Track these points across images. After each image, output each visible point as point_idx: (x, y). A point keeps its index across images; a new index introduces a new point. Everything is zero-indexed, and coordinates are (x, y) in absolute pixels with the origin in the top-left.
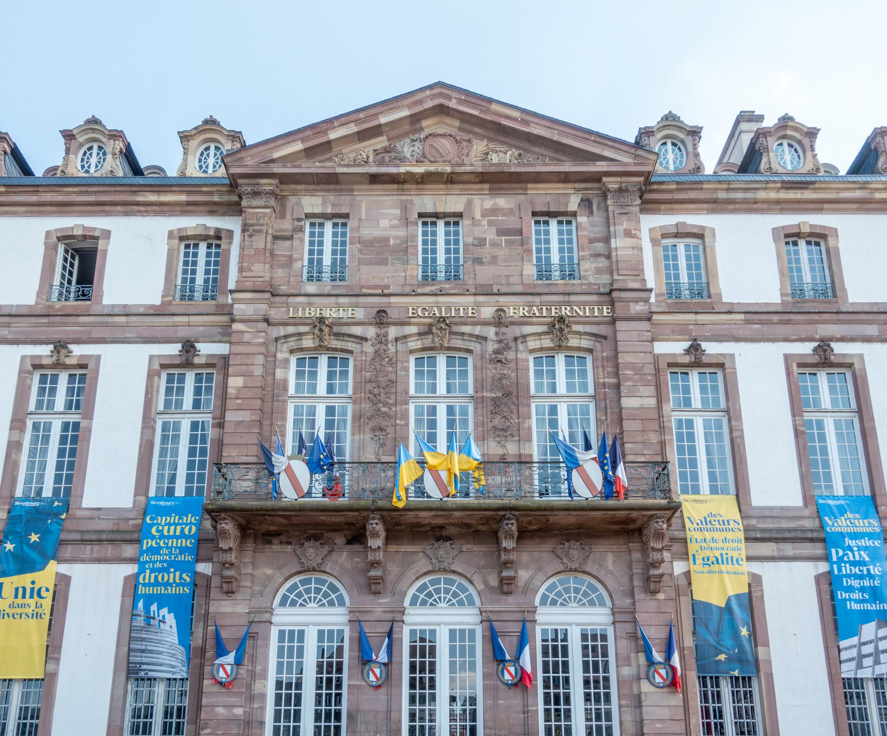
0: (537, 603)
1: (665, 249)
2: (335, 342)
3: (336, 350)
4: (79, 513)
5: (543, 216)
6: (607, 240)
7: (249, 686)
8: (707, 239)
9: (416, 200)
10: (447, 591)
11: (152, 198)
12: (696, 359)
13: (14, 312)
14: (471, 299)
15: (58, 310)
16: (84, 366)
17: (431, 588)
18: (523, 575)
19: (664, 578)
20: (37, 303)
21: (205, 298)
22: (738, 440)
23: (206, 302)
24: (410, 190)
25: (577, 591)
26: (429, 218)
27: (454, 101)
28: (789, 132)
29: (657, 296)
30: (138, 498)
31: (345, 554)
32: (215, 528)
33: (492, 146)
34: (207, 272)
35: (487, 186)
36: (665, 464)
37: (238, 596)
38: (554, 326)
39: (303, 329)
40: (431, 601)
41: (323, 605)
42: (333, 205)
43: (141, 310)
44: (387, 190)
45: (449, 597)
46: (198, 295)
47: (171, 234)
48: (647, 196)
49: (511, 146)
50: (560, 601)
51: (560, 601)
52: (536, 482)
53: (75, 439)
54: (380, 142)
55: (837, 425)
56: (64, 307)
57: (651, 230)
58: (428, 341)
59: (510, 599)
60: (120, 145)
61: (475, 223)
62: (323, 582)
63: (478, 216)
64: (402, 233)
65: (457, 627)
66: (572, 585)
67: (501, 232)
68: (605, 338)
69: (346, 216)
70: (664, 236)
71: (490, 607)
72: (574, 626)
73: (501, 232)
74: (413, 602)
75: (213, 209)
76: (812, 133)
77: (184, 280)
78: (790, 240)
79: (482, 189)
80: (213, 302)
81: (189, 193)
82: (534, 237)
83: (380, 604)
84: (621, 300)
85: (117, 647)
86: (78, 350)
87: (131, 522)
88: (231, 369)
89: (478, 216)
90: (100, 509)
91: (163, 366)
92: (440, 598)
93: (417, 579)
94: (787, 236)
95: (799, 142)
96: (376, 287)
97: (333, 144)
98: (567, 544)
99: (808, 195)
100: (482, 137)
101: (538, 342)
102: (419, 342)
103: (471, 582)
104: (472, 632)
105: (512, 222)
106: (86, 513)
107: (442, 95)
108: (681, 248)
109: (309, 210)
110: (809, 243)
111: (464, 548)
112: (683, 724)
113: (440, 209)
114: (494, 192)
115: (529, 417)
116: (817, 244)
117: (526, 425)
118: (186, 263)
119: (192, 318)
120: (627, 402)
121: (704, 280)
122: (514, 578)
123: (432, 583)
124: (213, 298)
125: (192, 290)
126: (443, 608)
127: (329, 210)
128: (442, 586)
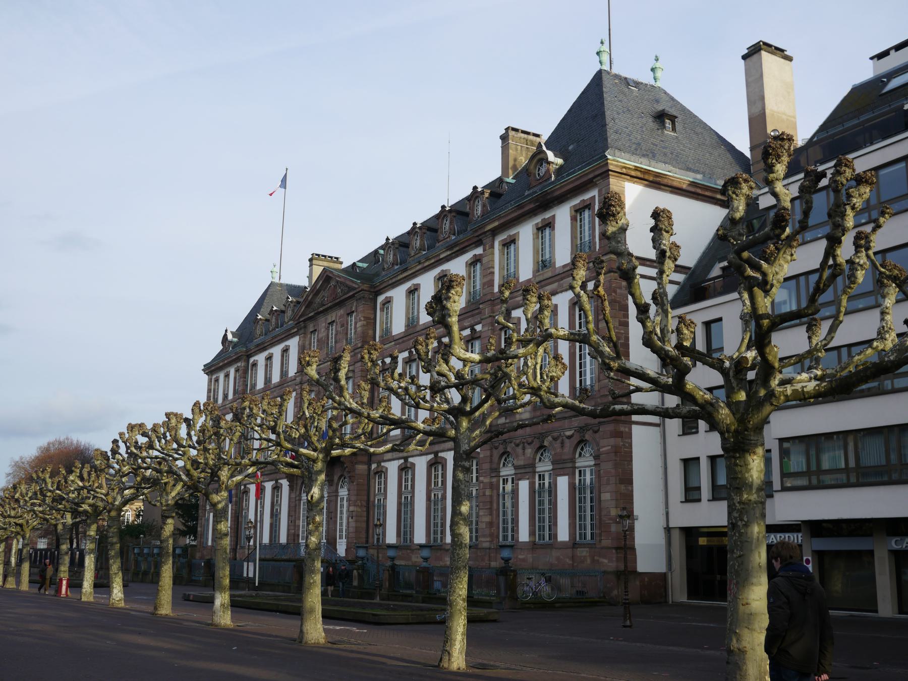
26: (332, 323)
99: (410, 272)
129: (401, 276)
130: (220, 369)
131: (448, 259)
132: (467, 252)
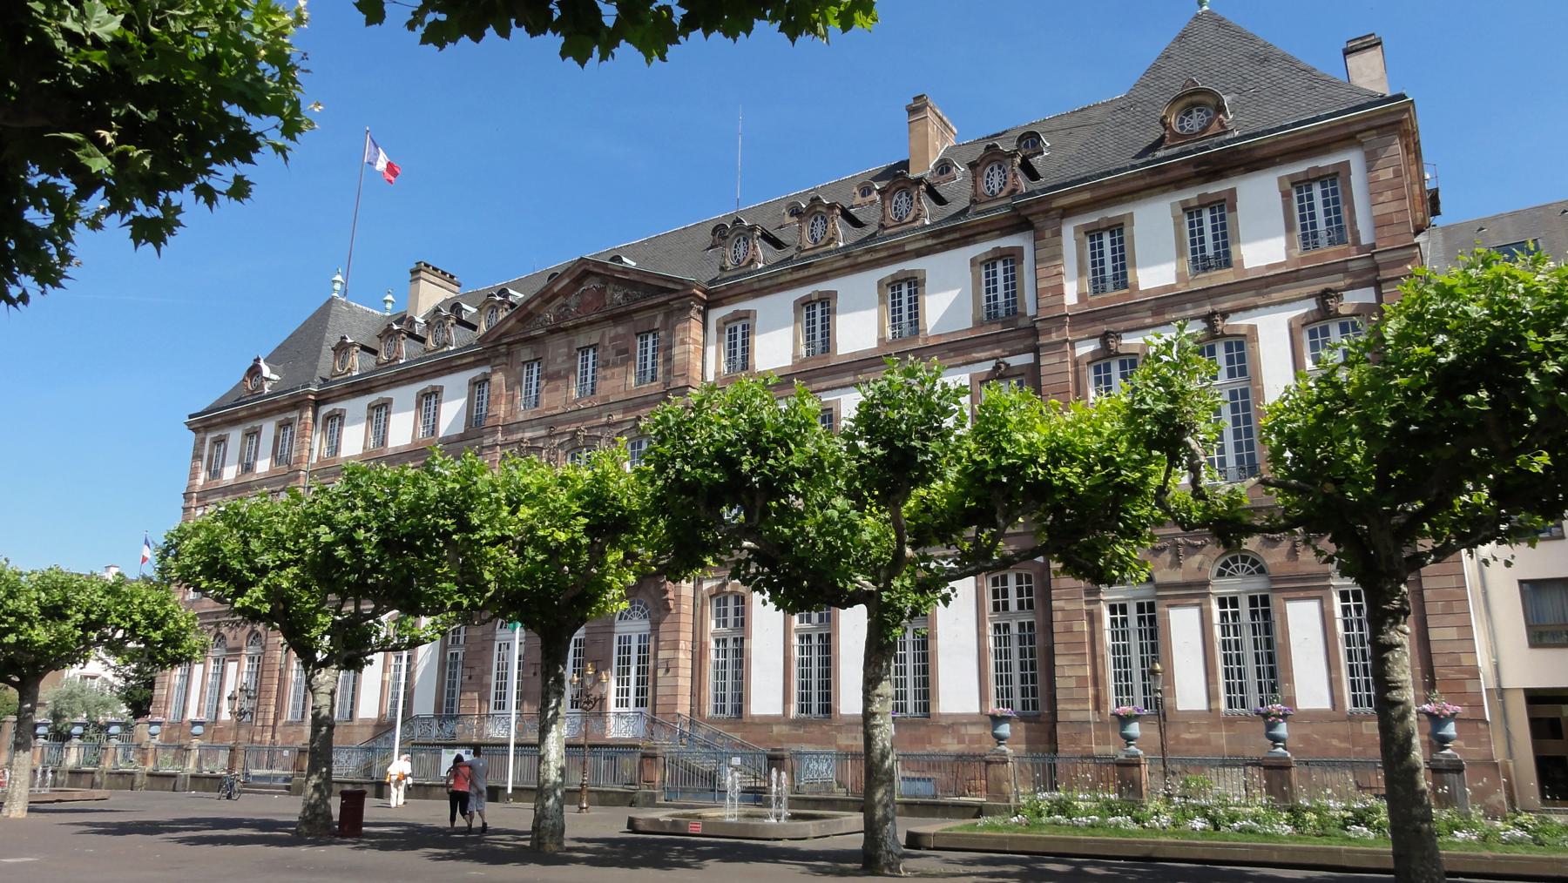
5: (642, 335)
26: (584, 350)
99: (813, 271)
114: (615, 326)
129: (789, 278)
130: (234, 422)
131: (919, 253)
132: (975, 242)
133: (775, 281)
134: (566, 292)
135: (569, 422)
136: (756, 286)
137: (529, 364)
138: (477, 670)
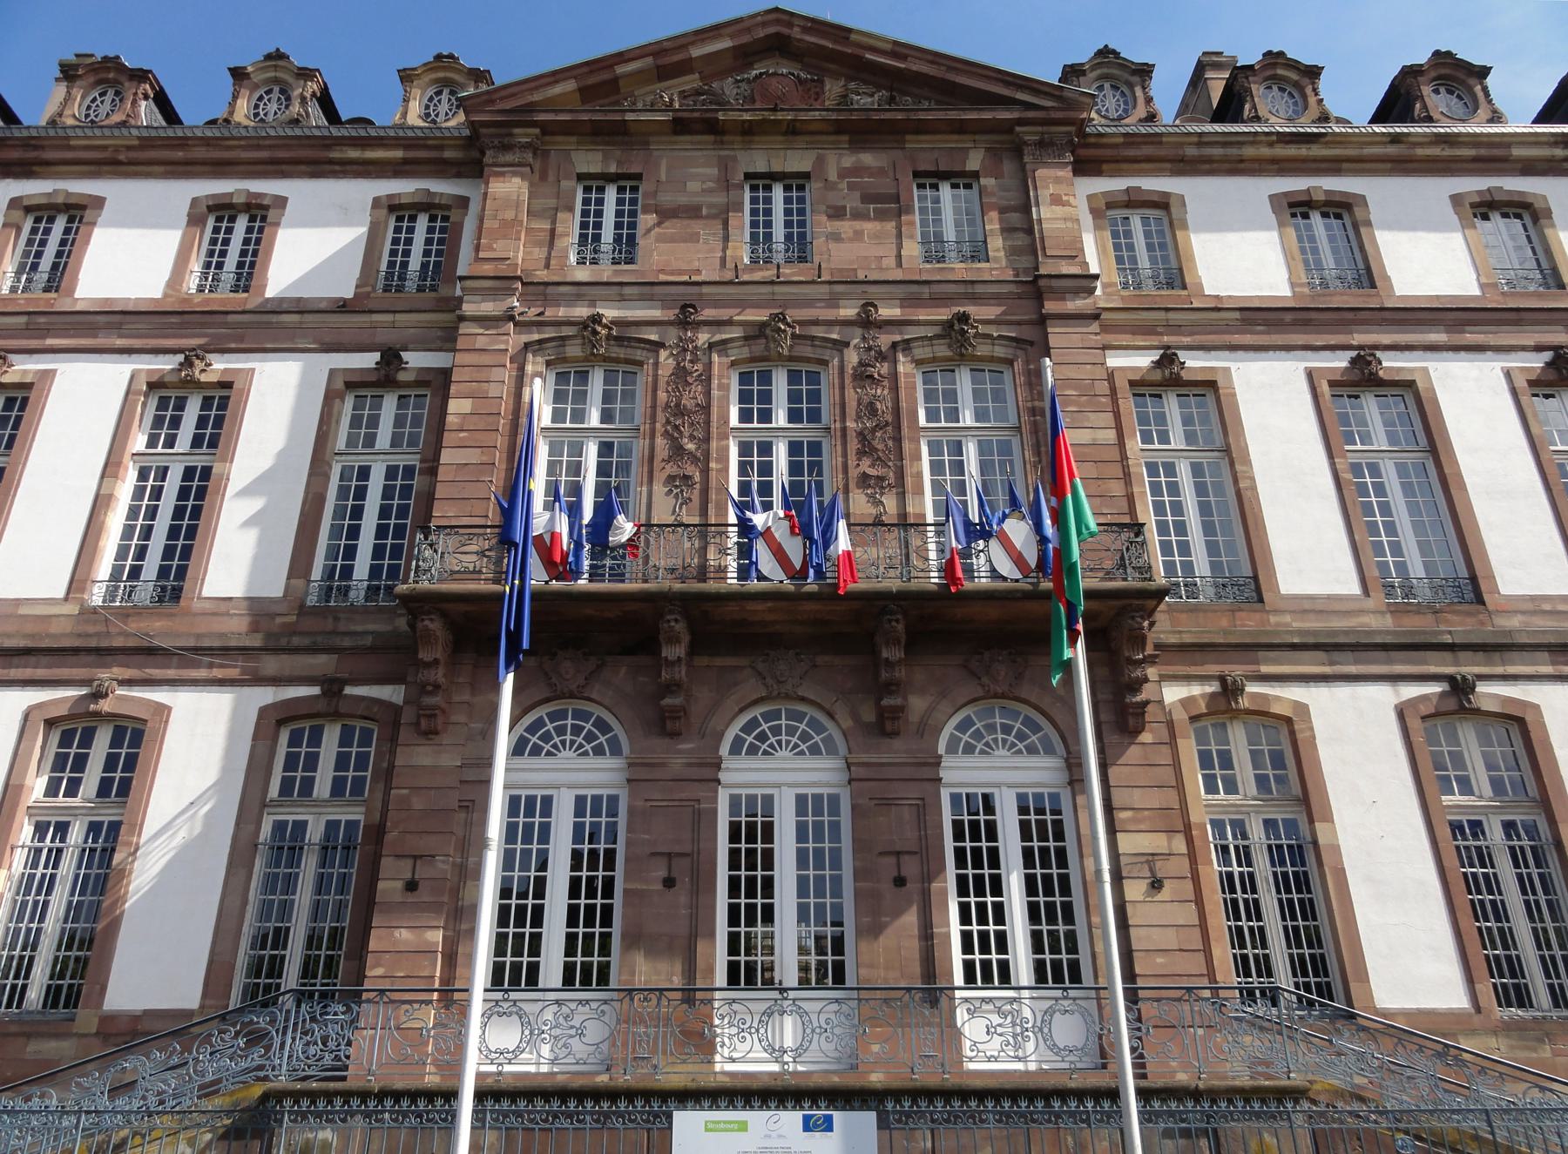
0: (941, 749)
1: (1114, 223)
2: (616, 349)
3: (617, 361)
4: (197, 605)
5: (930, 178)
6: (1026, 209)
7: (456, 892)
8: (1173, 210)
9: (742, 156)
10: (791, 731)
11: (353, 154)
12: (1167, 377)
13: (130, 308)
14: (826, 288)
15: (199, 304)
16: (228, 385)
17: (765, 726)
18: (917, 704)
19: (1149, 708)
20: (165, 295)
21: (420, 289)
22: (1249, 493)
23: (421, 295)
24: (732, 143)
25: (1007, 729)
26: (761, 181)
27: (796, 29)
28: (1280, 72)
29: (1104, 286)
30: (293, 581)
31: (623, 670)
32: (412, 626)
33: (852, 85)
34: (427, 253)
35: (846, 138)
36: (1138, 528)
37: (446, 739)
38: (952, 326)
39: (567, 331)
40: (764, 747)
41: (586, 754)
42: (619, 163)
43: (323, 306)
44: (699, 143)
45: (795, 740)
46: (411, 285)
47: (377, 203)
48: (1082, 152)
49: (879, 87)
50: (980, 746)
51: (980, 746)
52: (933, 555)
53: (201, 493)
54: (691, 82)
55: (1402, 470)
56: (207, 301)
57: (1090, 198)
58: (759, 348)
59: (897, 743)
60: (312, 87)
61: (829, 186)
62: (585, 716)
63: (833, 176)
64: (720, 199)
65: (810, 791)
66: (998, 720)
67: (867, 198)
68: (1032, 343)
69: (638, 177)
70: (1110, 206)
71: (865, 758)
72: (1004, 789)
73: (867, 198)
74: (736, 749)
75: (440, 168)
76: (1313, 72)
77: (391, 264)
78: (1298, 210)
79: (840, 142)
80: (433, 294)
81: (406, 147)
82: (917, 205)
83: (680, 752)
84: (1052, 290)
85: (237, 824)
86: (220, 365)
87: (279, 620)
88: (453, 389)
89: (833, 176)
90: (230, 599)
91: (350, 385)
92: (779, 742)
93: (741, 710)
94: (1291, 205)
95: (1296, 85)
96: (681, 272)
97: (621, 83)
98: (987, 655)
100: (836, 76)
101: (928, 349)
102: (746, 349)
103: (831, 716)
104: (834, 800)
105: (885, 186)
106: (207, 605)
107: (778, 22)
108: (1136, 224)
109: (584, 169)
110: (1325, 215)
111: (820, 660)
112: (1201, 957)
113: (777, 167)
115: (919, 458)
116: (1338, 216)
117: (915, 470)
118: (395, 241)
119: (399, 317)
120: (1071, 436)
121: (1174, 264)
122: (902, 709)
123: (767, 717)
124: (433, 289)
125: (402, 278)
126: (784, 759)
127: (613, 169)
128: (783, 722)
129: (1265, 151)
131: (1529, 168)
133: (1233, 151)
134: (714, 67)
135: (743, 304)
136: (1191, 151)
137: (594, 183)
138: (443, 866)
